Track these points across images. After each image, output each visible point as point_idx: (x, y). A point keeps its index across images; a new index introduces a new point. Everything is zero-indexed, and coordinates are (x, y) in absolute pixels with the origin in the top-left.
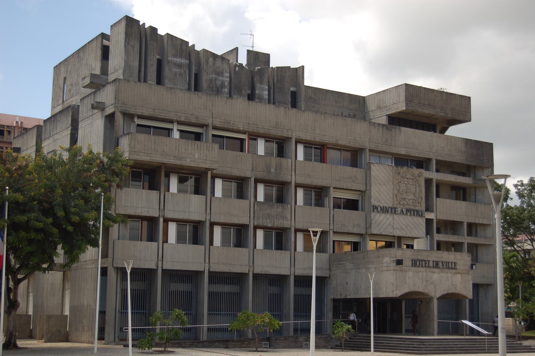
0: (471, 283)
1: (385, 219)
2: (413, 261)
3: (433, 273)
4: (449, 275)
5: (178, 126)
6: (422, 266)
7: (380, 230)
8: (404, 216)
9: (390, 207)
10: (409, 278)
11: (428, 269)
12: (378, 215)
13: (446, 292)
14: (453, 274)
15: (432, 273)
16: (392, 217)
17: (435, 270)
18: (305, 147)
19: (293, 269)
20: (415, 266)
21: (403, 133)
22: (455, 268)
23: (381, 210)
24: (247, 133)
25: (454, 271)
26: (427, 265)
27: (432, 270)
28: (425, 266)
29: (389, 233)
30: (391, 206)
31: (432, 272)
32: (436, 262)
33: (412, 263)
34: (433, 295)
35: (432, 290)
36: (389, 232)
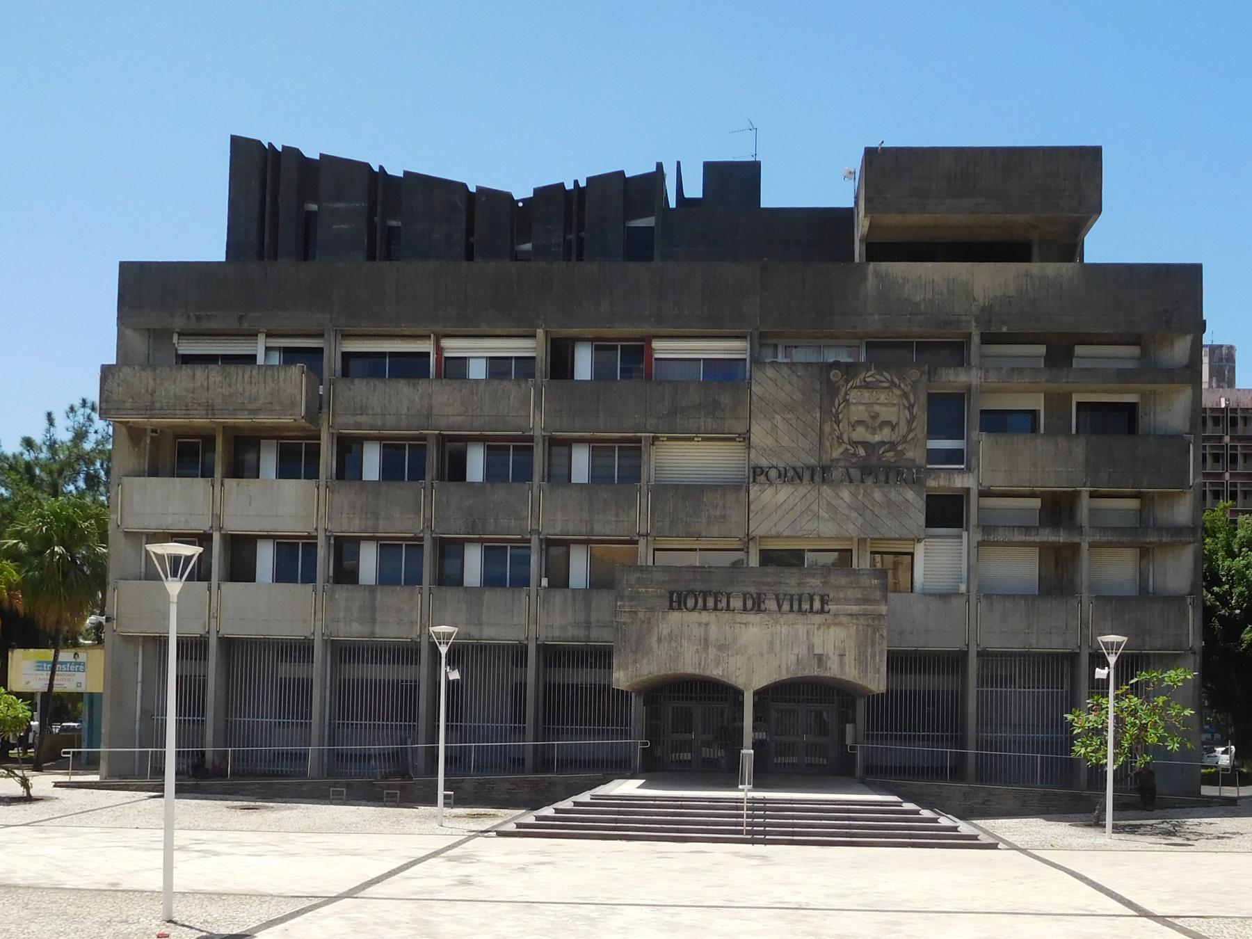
0: (885, 648)
1: (791, 498)
2: (675, 595)
3: (743, 626)
4: (802, 630)
5: (267, 340)
6: (705, 608)
7: (775, 525)
8: (853, 487)
9: (808, 468)
10: (659, 640)
11: (727, 616)
12: (769, 491)
13: (784, 676)
14: (816, 626)
15: (739, 625)
16: (815, 493)
17: (752, 617)
18: (597, 348)
19: (533, 627)
20: (679, 609)
21: (870, 277)
22: (822, 611)
23: (780, 477)
24: (432, 336)
25: (818, 619)
26: (720, 606)
27: (739, 618)
28: (716, 609)
29: (805, 533)
30: (813, 462)
31: (740, 623)
32: (755, 596)
33: (671, 601)
34: (739, 680)
35: (739, 669)
36: (804, 530)
